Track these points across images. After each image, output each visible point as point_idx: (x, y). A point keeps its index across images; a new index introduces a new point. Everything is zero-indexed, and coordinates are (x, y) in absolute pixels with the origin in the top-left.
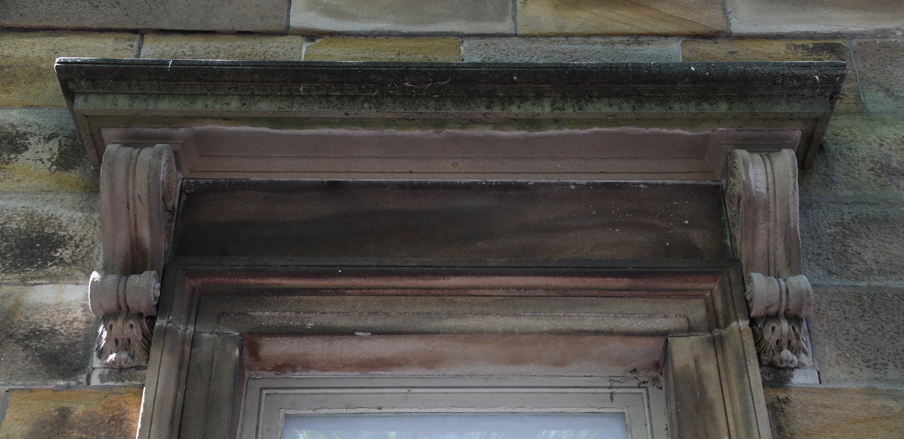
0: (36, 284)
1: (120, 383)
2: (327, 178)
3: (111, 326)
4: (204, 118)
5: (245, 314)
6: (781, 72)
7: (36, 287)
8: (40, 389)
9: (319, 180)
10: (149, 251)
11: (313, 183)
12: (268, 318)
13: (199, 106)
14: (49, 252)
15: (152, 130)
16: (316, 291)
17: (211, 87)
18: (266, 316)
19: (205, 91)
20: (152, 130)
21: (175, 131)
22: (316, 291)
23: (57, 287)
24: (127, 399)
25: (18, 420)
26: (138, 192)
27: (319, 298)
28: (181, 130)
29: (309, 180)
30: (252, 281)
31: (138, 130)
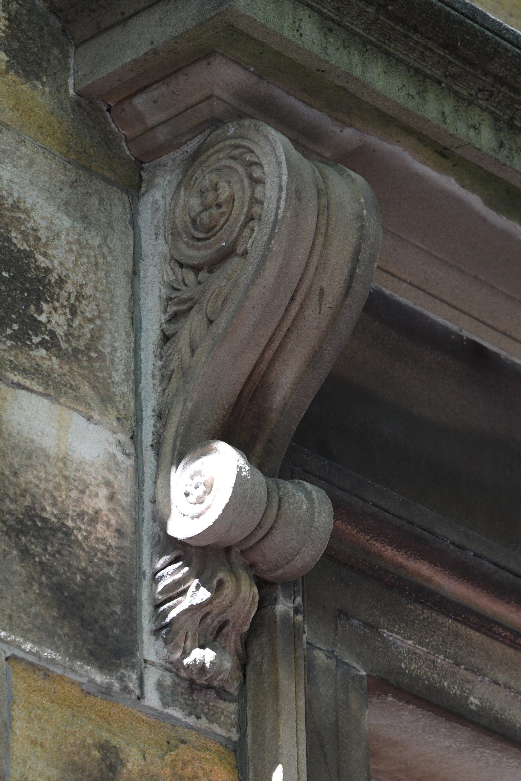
0: (20, 386)
1: (191, 720)
2: (469, 331)
3: (221, 583)
4: (408, 131)
5: (374, 628)
6: (288, 37)
7: (22, 393)
8: (62, 677)
9: (455, 328)
10: (274, 416)
11: (446, 332)
12: (413, 656)
13: (432, 108)
14: (27, 302)
15: (300, 107)
16: (486, 624)
17: (453, 70)
18: (407, 647)
19: (438, 73)
20: (300, 107)
21: (337, 130)
22: (486, 624)
23: (57, 409)
24: (207, 767)
25: (37, 748)
26: (324, 284)
27: (486, 641)
28: (348, 132)
29: (440, 320)
30: (389, 552)
31: (278, 92)
